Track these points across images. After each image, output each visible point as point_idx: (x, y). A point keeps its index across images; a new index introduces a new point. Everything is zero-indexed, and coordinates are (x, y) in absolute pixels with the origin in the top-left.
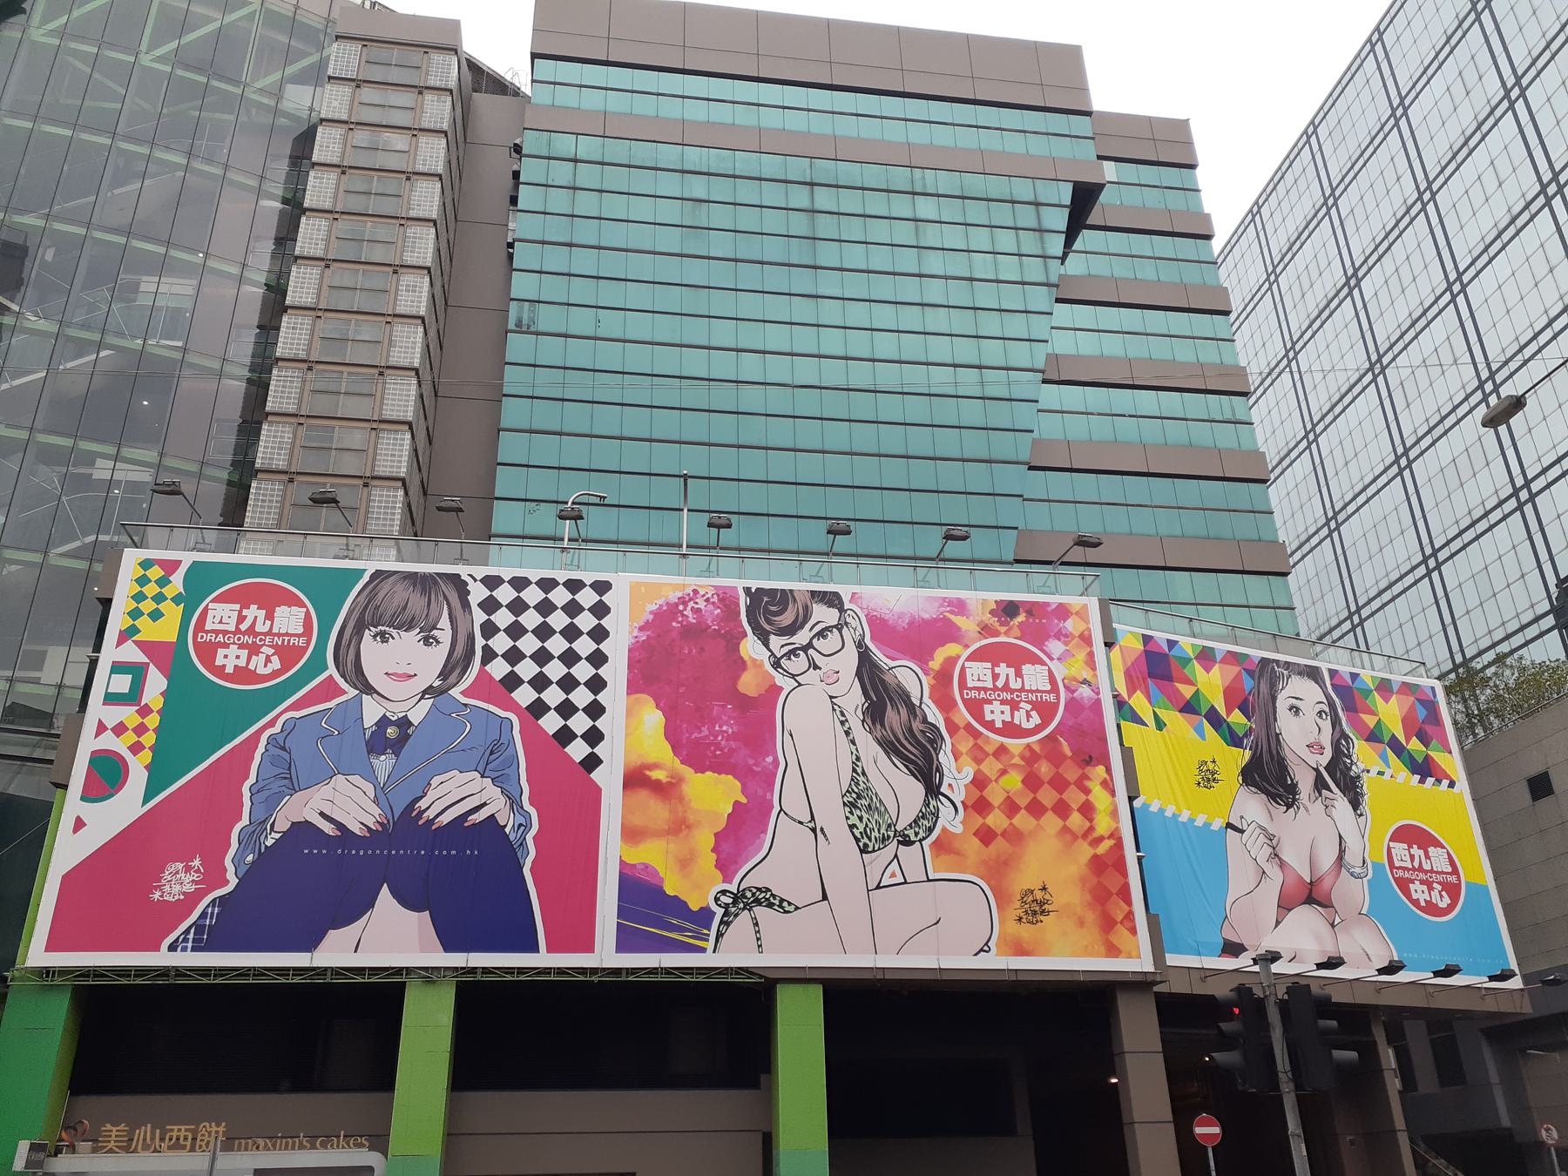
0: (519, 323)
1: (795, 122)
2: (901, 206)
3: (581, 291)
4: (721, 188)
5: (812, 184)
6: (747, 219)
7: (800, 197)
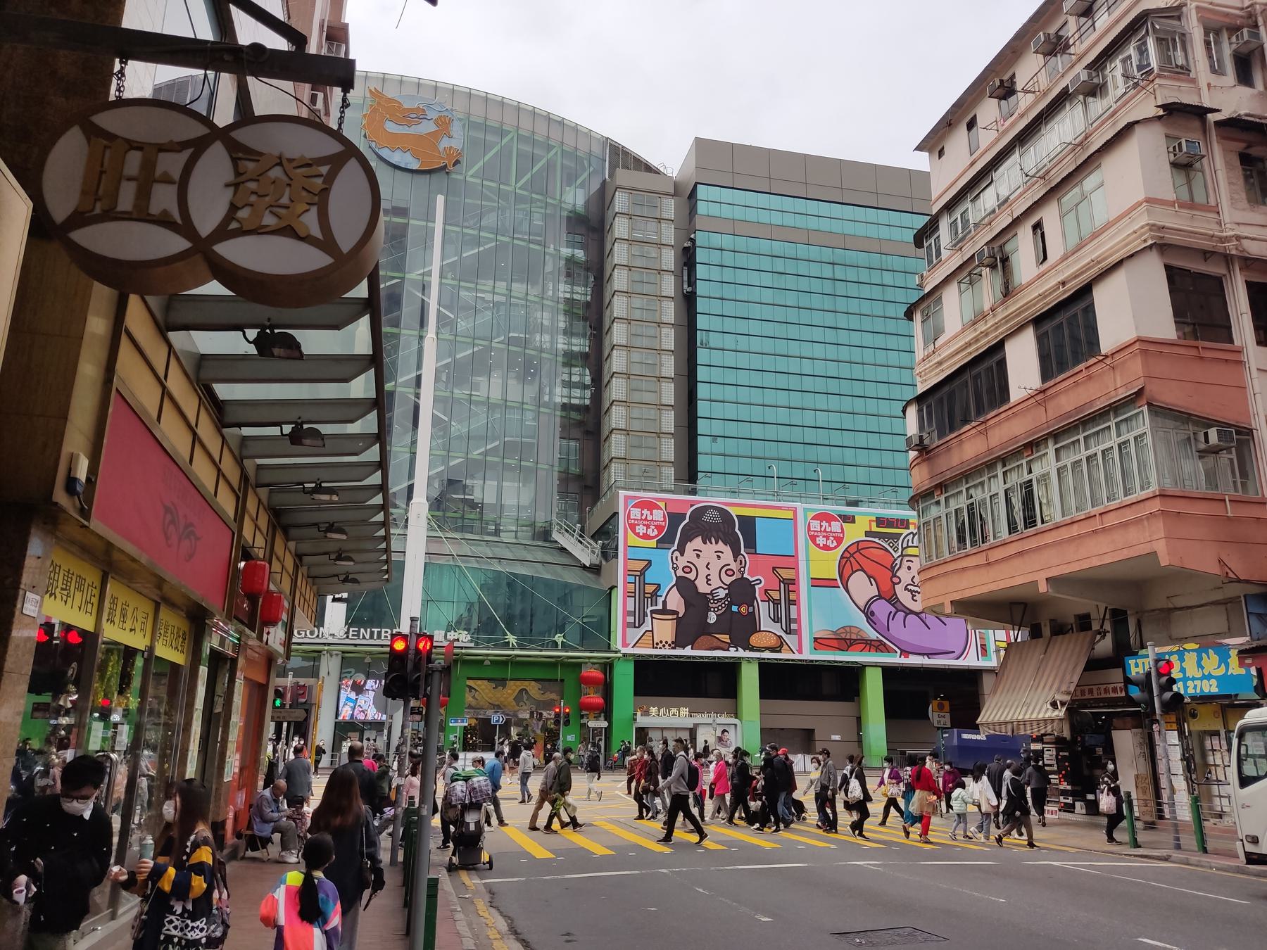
0: (702, 344)
1: (825, 225)
2: (876, 277)
3: (729, 325)
4: (790, 267)
5: (833, 264)
6: (804, 284)
7: (828, 271)
